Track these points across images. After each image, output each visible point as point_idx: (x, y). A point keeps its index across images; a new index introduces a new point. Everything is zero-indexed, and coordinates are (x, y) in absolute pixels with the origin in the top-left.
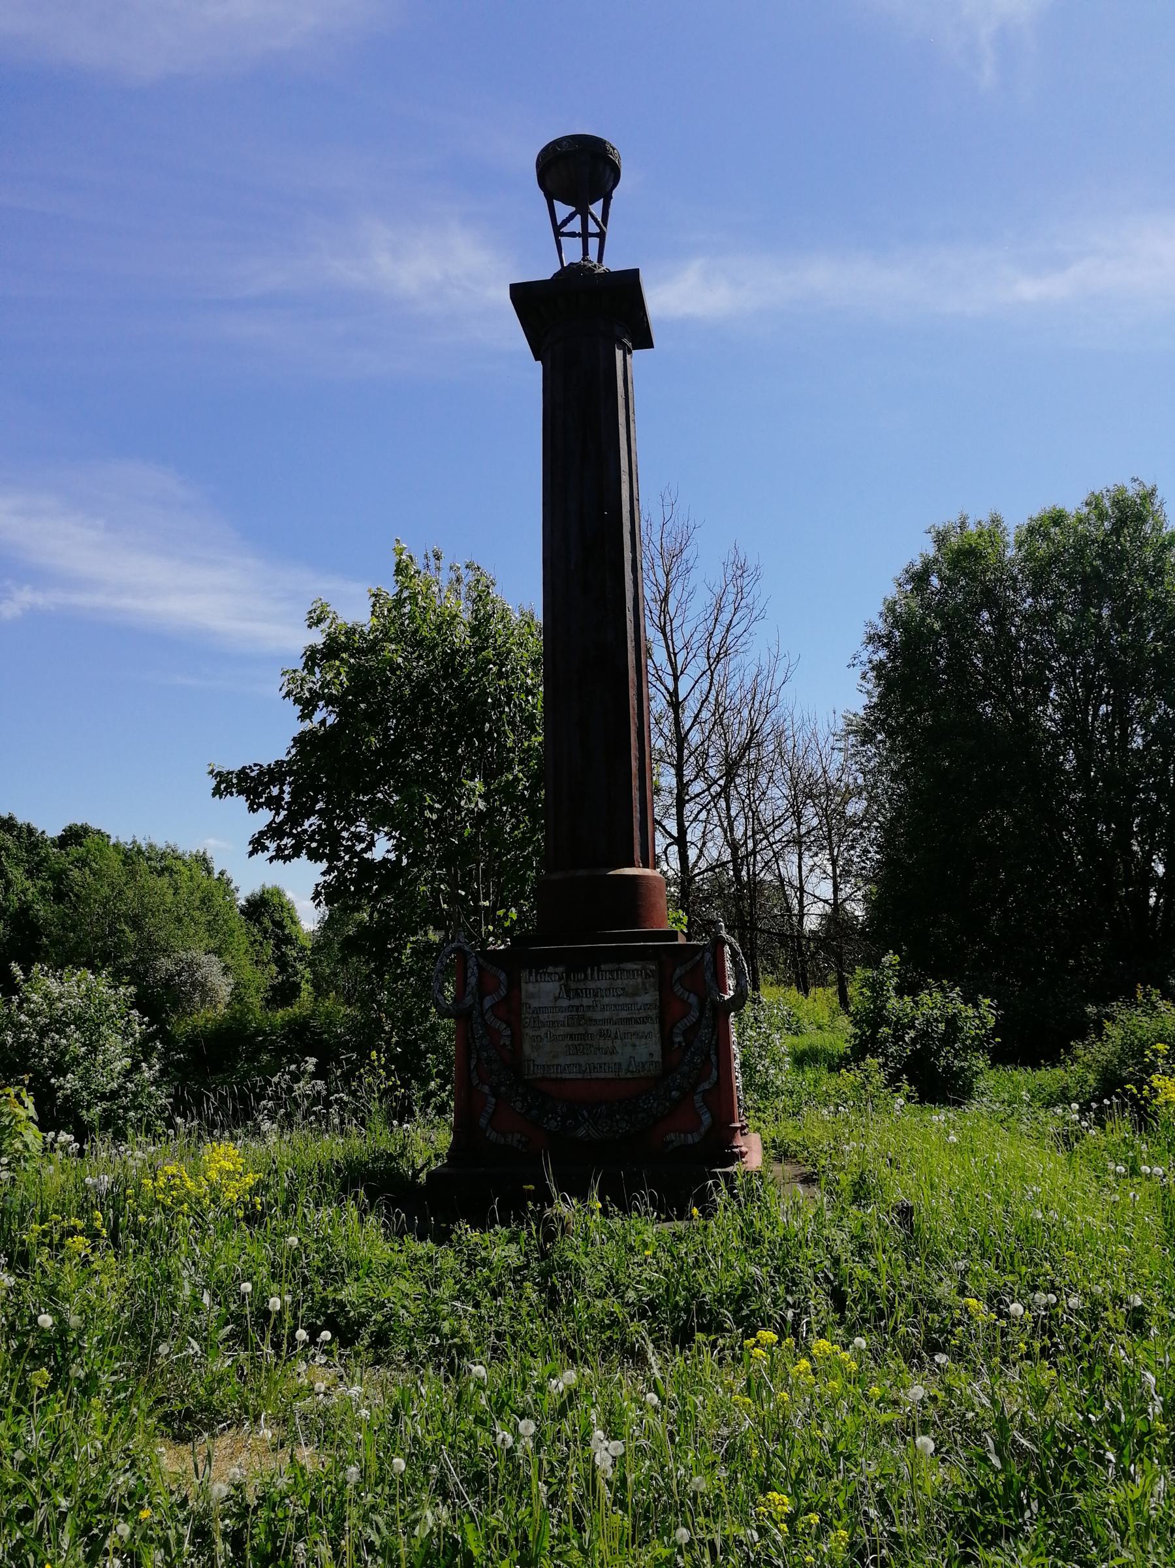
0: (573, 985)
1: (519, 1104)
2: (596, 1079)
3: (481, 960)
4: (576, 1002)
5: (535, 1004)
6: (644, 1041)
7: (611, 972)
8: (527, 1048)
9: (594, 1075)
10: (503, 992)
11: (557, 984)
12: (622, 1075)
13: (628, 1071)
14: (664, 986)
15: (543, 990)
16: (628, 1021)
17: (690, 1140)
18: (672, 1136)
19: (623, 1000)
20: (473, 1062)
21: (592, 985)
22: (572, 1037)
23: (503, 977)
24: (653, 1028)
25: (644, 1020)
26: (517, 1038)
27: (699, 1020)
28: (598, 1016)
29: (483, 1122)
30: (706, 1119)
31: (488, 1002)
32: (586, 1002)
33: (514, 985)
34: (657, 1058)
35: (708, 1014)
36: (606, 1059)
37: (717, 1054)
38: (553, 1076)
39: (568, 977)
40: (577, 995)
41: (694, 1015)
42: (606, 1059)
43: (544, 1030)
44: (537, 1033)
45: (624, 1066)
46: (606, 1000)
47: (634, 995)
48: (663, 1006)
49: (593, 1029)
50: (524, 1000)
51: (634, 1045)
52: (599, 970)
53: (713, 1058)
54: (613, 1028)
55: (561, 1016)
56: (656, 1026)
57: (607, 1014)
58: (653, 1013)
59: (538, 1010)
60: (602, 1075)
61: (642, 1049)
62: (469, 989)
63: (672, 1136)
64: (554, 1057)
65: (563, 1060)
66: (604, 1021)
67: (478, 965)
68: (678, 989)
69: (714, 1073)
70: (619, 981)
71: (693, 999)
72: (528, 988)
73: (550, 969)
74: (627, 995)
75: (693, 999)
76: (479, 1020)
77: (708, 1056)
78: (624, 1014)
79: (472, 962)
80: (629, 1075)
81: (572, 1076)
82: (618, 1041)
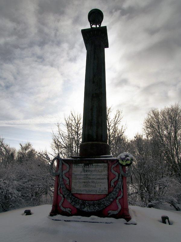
0: (86, 169)
1: (70, 200)
2: (91, 194)
3: (63, 162)
5: (76, 173)
6: (103, 184)
7: (95, 166)
8: (73, 185)
9: (90, 193)
10: (68, 170)
11: (82, 168)
12: (97, 193)
13: (99, 192)
14: (109, 170)
15: (78, 170)
16: (98, 179)
17: (115, 213)
18: (110, 212)
19: (98, 173)
20: (59, 188)
21: (90, 169)
22: (85, 182)
26: (70, 182)
27: (118, 179)
28: (91, 177)
29: (60, 205)
30: (120, 207)
31: (64, 172)
32: (89, 173)
33: (70, 168)
34: (107, 189)
35: (121, 178)
36: (94, 189)
37: (123, 189)
38: (79, 193)
39: (84, 166)
40: (87, 172)
41: (117, 178)
42: (94, 189)
43: (77, 181)
44: (75, 181)
45: (98, 191)
46: (94, 173)
47: (101, 172)
48: (108, 175)
49: (90, 181)
50: (73, 172)
51: (101, 185)
52: (92, 165)
53: (122, 190)
54: (95, 181)
55: (82, 177)
56: (107, 180)
57: (94, 177)
58: (106, 177)
59: (76, 175)
60: (91, 193)
61: (102, 187)
62: (59, 169)
63: (109, 212)
64: (80, 188)
65: (82, 189)
66: (93, 179)
67: (63, 163)
68: (112, 171)
70: (97, 168)
71: (117, 174)
73: (80, 165)
74: (99, 172)
76: (61, 177)
77: (120, 189)
78: (98, 177)
79: (60, 162)
80: (99, 194)
81: (84, 193)
82: (97, 184)
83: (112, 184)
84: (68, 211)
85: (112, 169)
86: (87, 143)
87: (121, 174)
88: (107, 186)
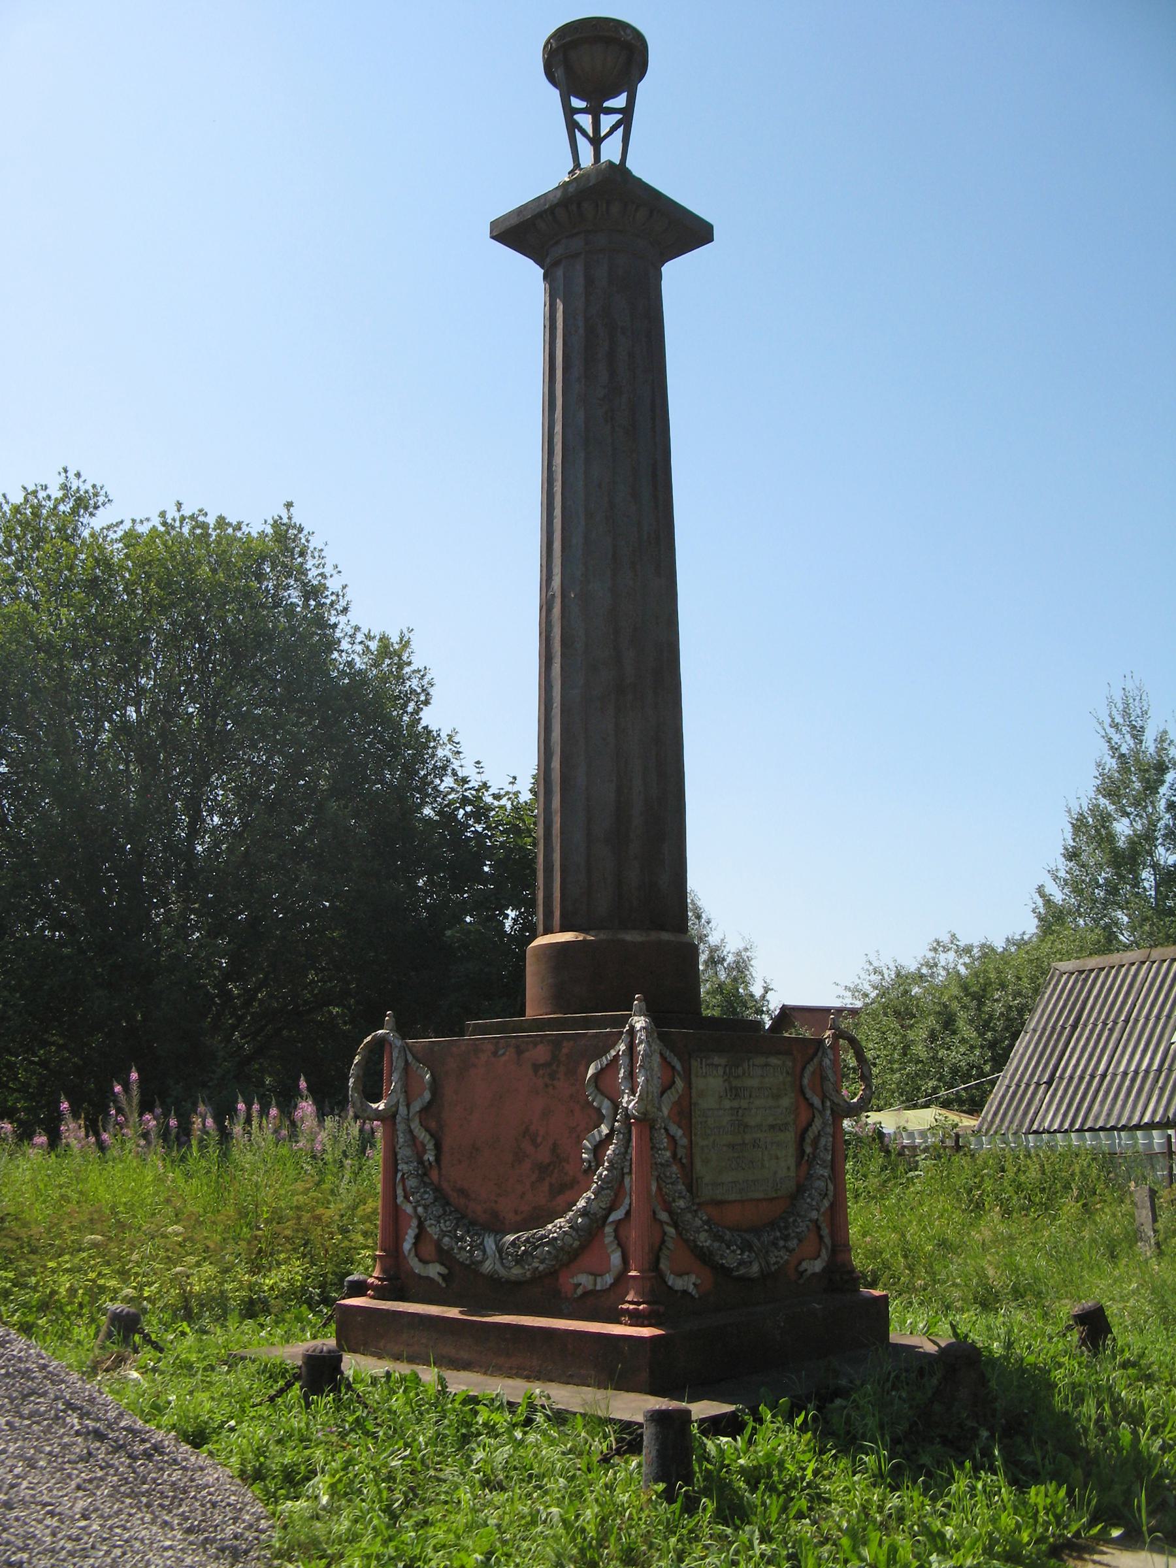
0: (735, 1083)
1: (703, 1236)
4: (735, 1104)
8: (698, 1165)
16: (772, 1127)
23: (678, 1066)
24: (789, 1136)
25: (783, 1128)
30: (827, 1240)
32: (744, 1103)
49: (748, 1137)
69: (831, 1187)
72: (699, 1083)
73: (716, 1060)
75: (817, 1101)
78: (771, 1121)
83: (808, 1150)
84: (691, 1288)
85: (805, 1081)
86: (654, 936)
87: (828, 1104)
88: (792, 1162)
